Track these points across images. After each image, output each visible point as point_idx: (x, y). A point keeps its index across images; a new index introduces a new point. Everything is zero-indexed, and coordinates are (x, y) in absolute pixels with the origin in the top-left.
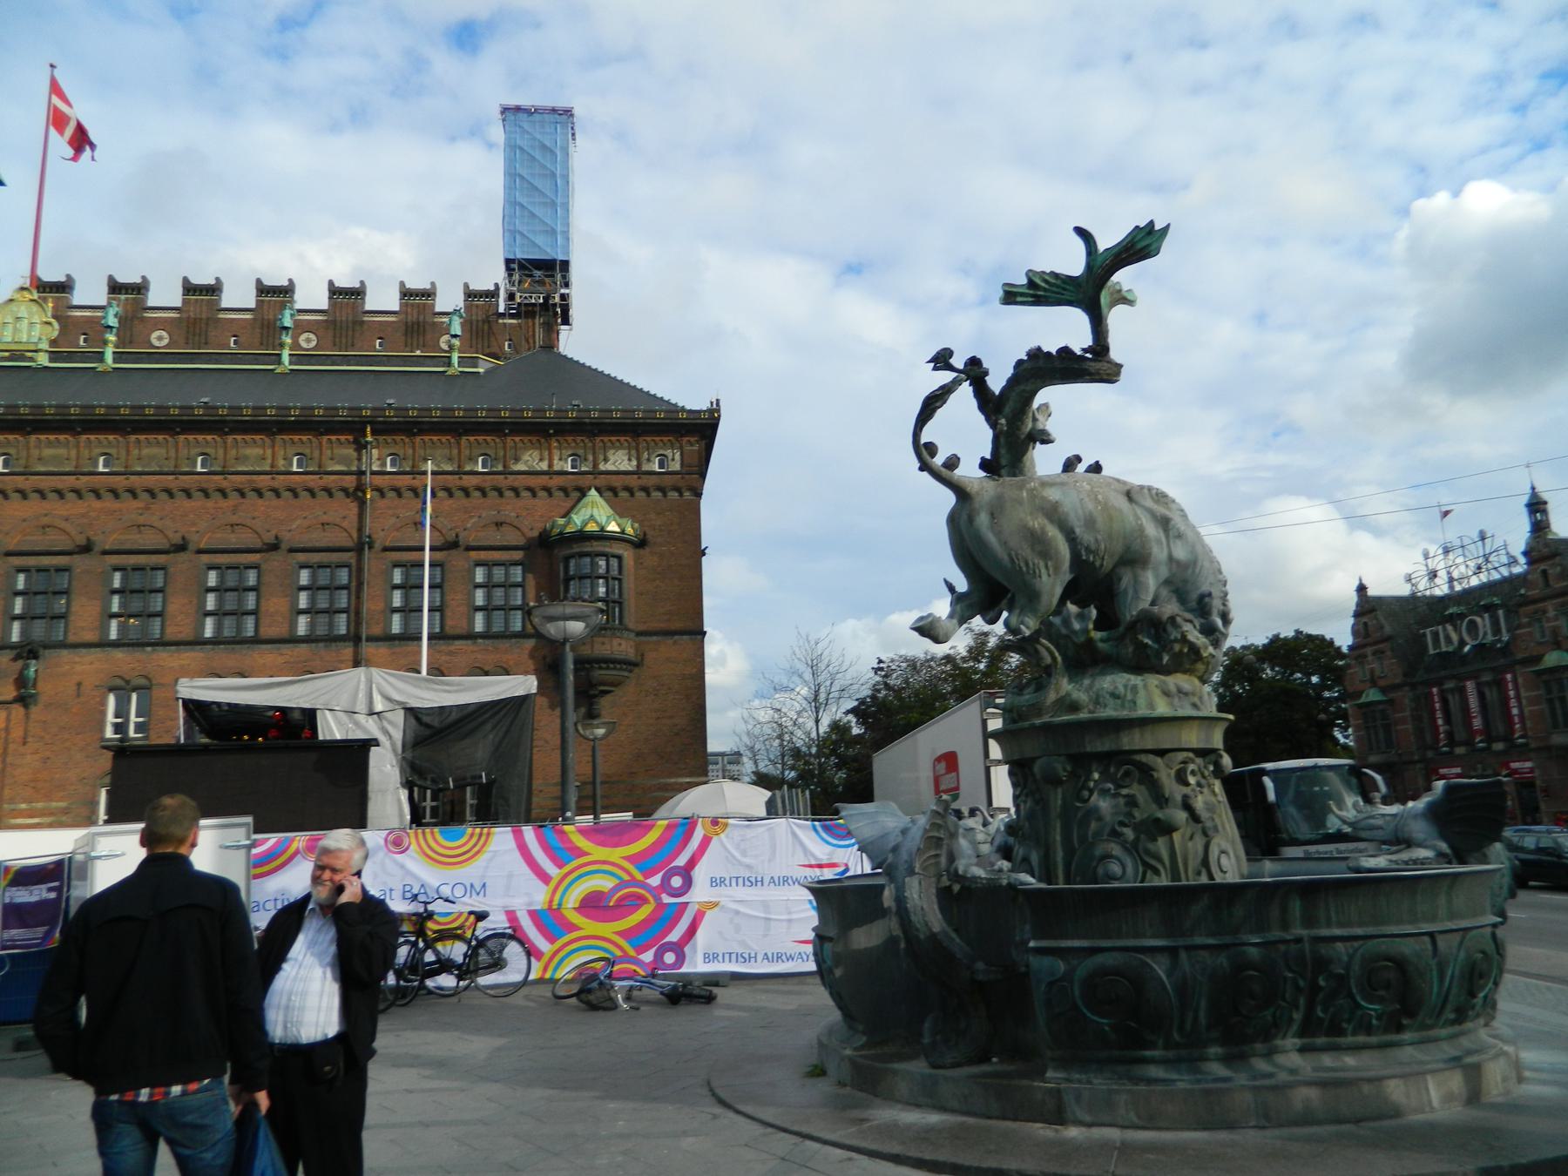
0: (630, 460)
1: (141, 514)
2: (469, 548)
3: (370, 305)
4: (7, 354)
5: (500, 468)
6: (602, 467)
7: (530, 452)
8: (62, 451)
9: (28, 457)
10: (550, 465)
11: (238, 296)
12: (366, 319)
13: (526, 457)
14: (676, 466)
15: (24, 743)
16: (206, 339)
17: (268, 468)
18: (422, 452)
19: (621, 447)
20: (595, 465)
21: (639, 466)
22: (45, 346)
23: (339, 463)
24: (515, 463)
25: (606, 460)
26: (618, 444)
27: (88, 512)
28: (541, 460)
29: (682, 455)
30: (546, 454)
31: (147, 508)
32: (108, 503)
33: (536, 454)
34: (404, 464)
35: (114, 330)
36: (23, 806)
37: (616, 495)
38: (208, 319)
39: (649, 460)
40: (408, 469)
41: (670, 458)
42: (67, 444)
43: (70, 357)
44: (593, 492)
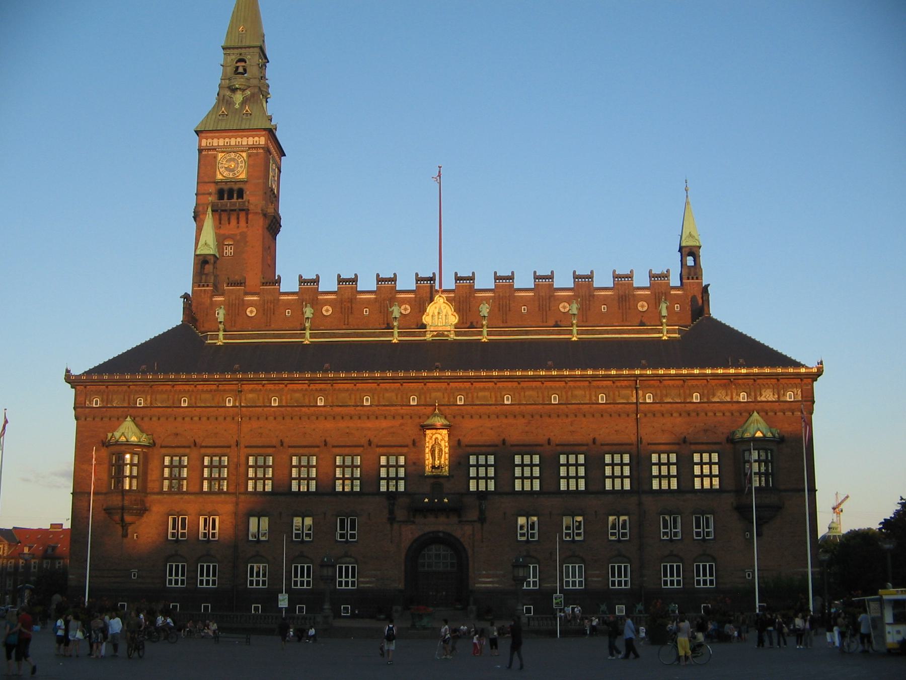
0: (774, 394)
1: (527, 426)
2: (691, 444)
3: (596, 284)
4: (435, 333)
5: (705, 400)
6: (759, 399)
7: (720, 391)
8: (487, 394)
9: (473, 397)
10: (732, 398)
11: (524, 281)
12: (595, 293)
13: (719, 394)
14: (800, 399)
15: (482, 542)
16: (509, 308)
17: (588, 402)
18: (664, 392)
19: (769, 388)
20: (755, 398)
21: (779, 397)
22: (452, 329)
23: (623, 398)
24: (713, 397)
25: (761, 395)
26: (766, 386)
27: (501, 425)
28: (727, 395)
29: (802, 391)
30: (729, 392)
31: (529, 423)
32: (511, 420)
33: (724, 392)
34: (655, 398)
35: (486, 318)
36: (484, 572)
37: (767, 414)
38: (509, 296)
39: (784, 395)
40: (657, 401)
41: (796, 393)
42: (488, 389)
43: (465, 334)
44: (755, 414)
